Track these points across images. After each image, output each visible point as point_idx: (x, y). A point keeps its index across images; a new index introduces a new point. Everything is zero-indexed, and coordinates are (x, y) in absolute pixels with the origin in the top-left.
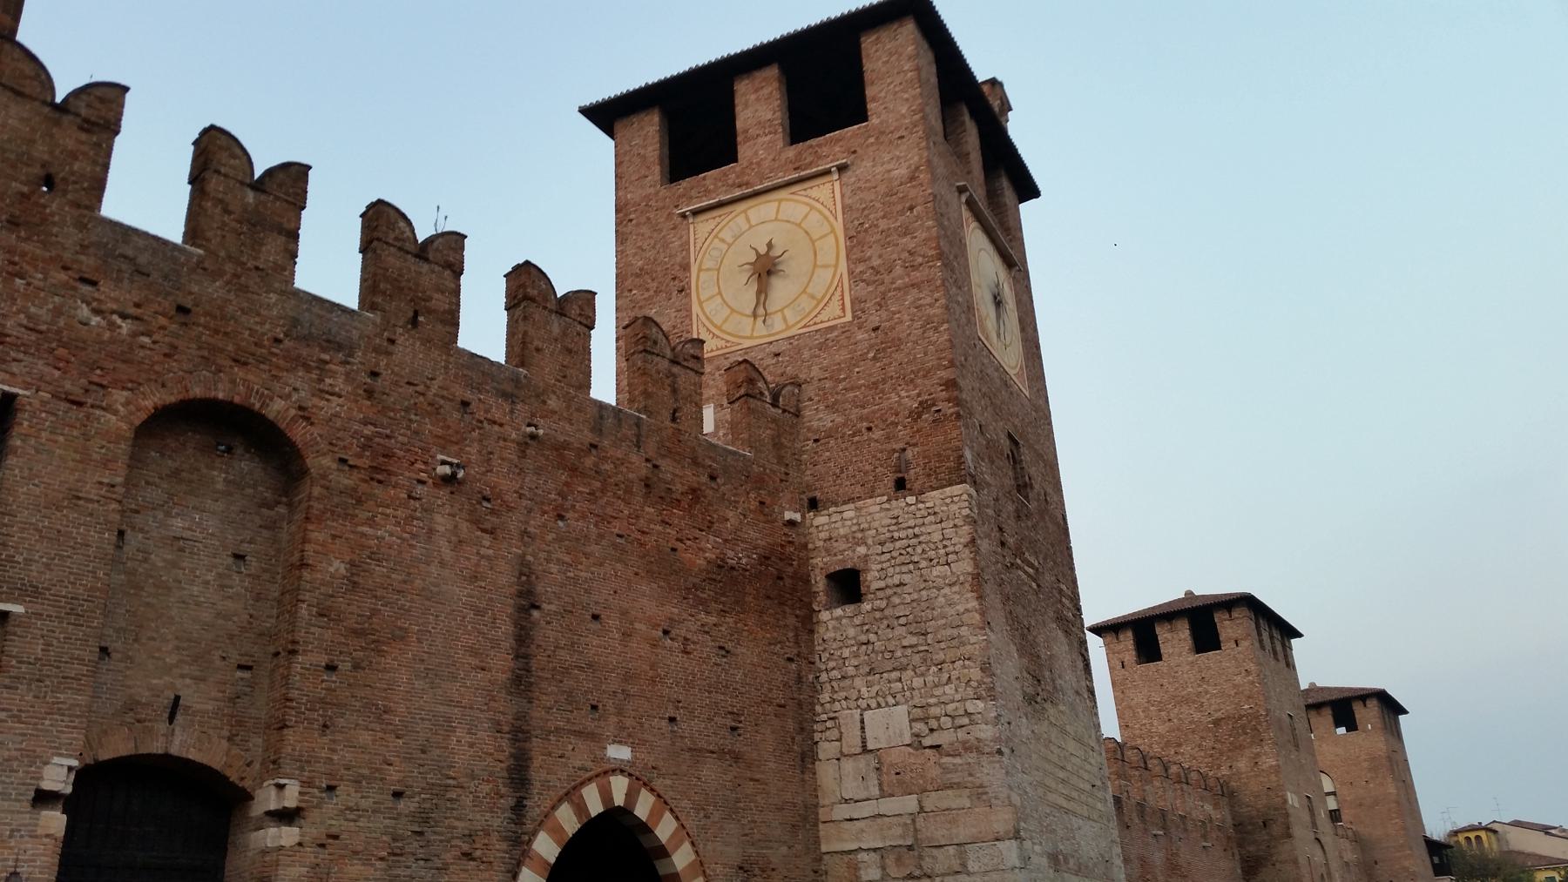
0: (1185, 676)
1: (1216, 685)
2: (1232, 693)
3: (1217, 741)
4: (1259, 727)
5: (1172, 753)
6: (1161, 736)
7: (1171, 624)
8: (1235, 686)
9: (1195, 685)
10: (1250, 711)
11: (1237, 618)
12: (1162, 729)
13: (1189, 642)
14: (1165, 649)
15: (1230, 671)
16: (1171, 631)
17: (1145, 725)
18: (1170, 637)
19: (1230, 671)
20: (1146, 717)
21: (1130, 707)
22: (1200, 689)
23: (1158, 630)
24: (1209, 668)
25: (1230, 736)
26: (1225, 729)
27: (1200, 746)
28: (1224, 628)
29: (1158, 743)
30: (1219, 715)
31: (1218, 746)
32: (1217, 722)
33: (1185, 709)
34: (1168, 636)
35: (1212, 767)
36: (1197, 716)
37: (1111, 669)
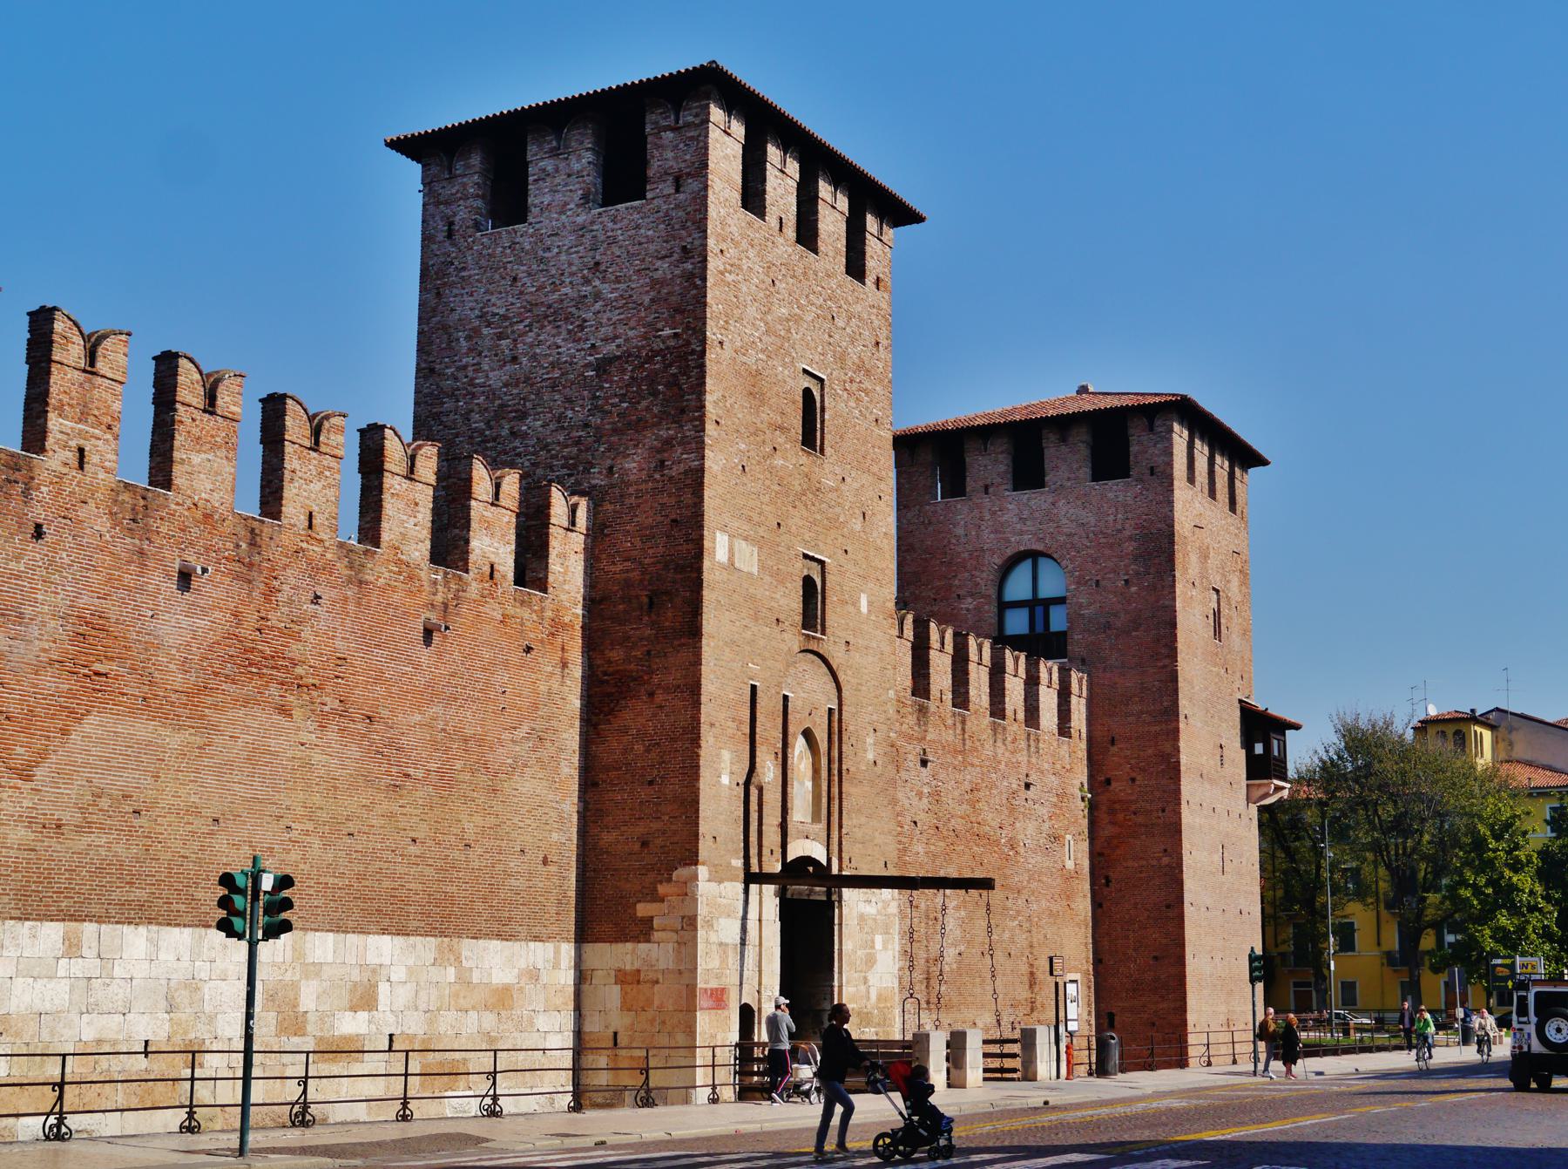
1: (618, 280)
2: (647, 300)
3: (596, 409)
4: (683, 379)
5: (505, 432)
6: (492, 394)
7: (559, 139)
8: (654, 283)
9: (577, 279)
10: (672, 343)
11: (688, 125)
12: (496, 378)
13: (592, 179)
14: (538, 196)
15: (652, 247)
16: (554, 153)
17: (465, 367)
18: (550, 168)
19: (652, 247)
20: (470, 350)
21: (445, 328)
22: (586, 289)
23: (532, 151)
24: (613, 241)
25: (623, 398)
27: (560, 418)
28: (658, 147)
29: (482, 411)
31: (596, 420)
32: (603, 367)
34: (549, 165)
35: (575, 466)
36: (568, 349)
37: (427, 239)
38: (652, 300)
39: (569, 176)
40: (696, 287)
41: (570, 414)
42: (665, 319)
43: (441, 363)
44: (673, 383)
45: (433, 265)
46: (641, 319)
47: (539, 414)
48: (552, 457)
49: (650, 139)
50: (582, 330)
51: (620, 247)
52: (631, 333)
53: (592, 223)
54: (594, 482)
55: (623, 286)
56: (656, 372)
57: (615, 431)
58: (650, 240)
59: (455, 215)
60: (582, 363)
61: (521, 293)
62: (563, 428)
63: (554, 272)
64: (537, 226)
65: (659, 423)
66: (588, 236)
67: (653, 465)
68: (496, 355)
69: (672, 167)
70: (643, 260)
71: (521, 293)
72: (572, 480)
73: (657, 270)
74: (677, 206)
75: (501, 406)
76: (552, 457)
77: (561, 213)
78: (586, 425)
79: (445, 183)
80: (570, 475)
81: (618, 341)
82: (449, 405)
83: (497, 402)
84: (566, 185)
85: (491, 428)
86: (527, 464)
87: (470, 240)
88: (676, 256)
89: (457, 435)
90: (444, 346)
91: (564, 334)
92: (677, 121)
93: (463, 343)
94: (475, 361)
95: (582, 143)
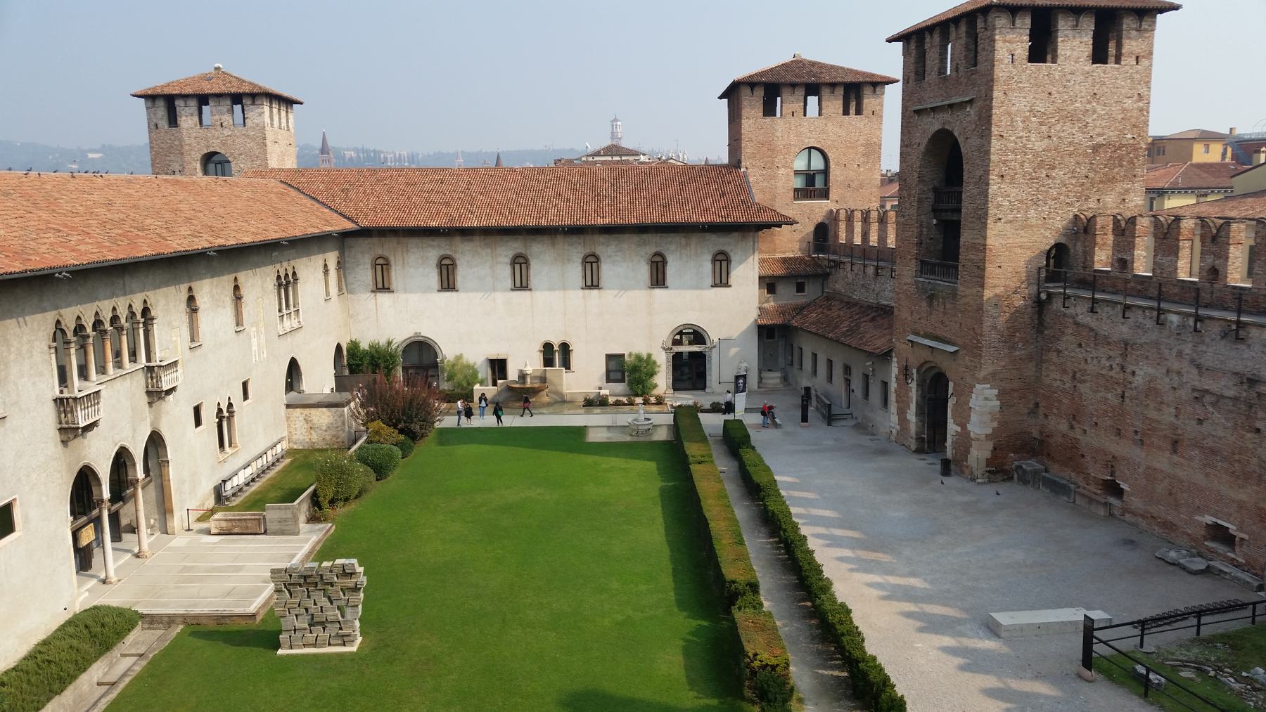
0: (1077, 86)
1: (1105, 105)
2: (1120, 117)
4: (1135, 160)
5: (1044, 175)
6: (1036, 155)
8: (1124, 110)
9: (1084, 100)
10: (1131, 141)
17: (1021, 137)
19: (1123, 91)
21: (1009, 114)
22: (1088, 107)
26: (1103, 156)
30: (1100, 140)
32: (1096, 148)
33: (1068, 126)
35: (1080, 197)
36: (1079, 136)
38: (1123, 119)
39: (1081, 43)
40: (1144, 116)
41: (1078, 170)
42: (1128, 129)
43: (1007, 133)
44: (1131, 162)
45: (1002, 77)
46: (1116, 127)
47: (1062, 168)
48: (1069, 191)
49: (1124, 32)
50: (1086, 128)
51: (1107, 88)
52: (1111, 134)
53: (1093, 72)
54: (1090, 206)
55: (1108, 108)
56: (1123, 155)
57: (1101, 182)
58: (1123, 87)
59: (1015, 50)
60: (1085, 145)
61: (1053, 102)
62: (1074, 177)
63: (1072, 94)
64: (1063, 67)
65: (1123, 181)
66: (1091, 78)
67: (1119, 201)
68: (1039, 133)
69: (1134, 50)
70: (1119, 97)
71: (1053, 102)
72: (1079, 204)
73: (1125, 103)
74: (1137, 72)
75: (1042, 161)
76: (1069, 191)
77: (1076, 62)
78: (1087, 177)
79: (1009, 30)
80: (1078, 201)
81: (1104, 137)
82: (1011, 157)
83: (1039, 159)
84: (1079, 47)
85: (1035, 172)
86: (1055, 193)
87: (1024, 66)
88: (1135, 98)
89: (1016, 174)
90: (1008, 124)
91: (1077, 129)
92: (1140, 27)
93: (1021, 124)
94: (1027, 135)
95: (1089, 26)
